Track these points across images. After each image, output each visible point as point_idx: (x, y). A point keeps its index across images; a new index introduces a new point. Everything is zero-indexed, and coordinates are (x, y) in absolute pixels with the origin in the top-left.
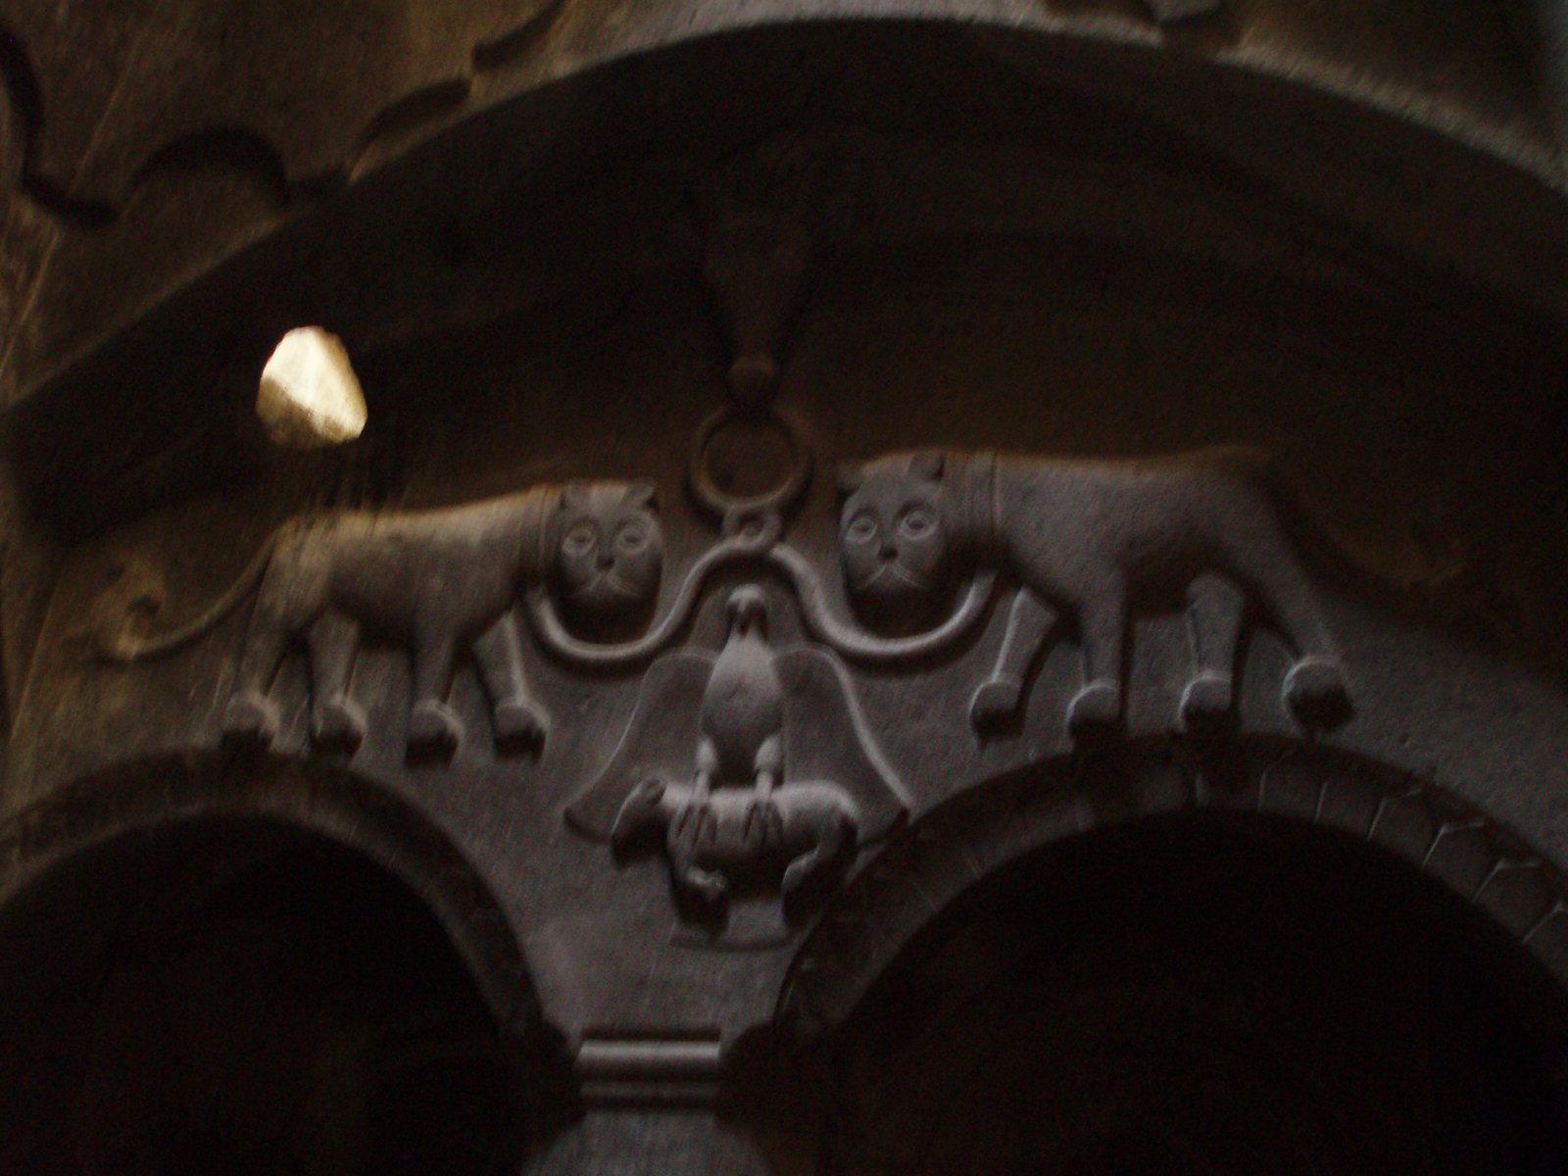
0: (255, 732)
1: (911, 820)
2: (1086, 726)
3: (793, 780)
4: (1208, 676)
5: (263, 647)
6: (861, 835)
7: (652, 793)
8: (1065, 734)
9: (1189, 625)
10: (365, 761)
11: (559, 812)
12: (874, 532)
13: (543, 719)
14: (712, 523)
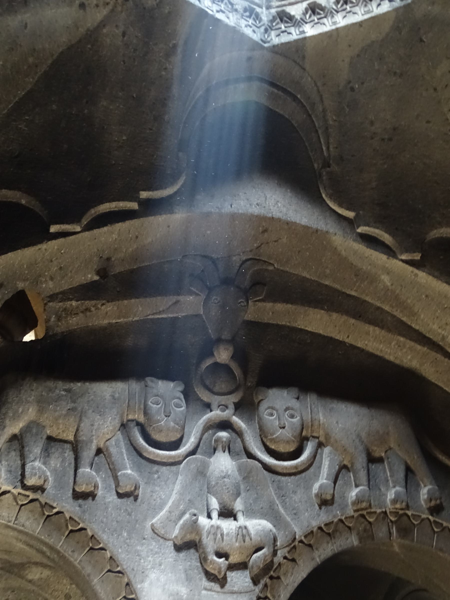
11: (148, 525)
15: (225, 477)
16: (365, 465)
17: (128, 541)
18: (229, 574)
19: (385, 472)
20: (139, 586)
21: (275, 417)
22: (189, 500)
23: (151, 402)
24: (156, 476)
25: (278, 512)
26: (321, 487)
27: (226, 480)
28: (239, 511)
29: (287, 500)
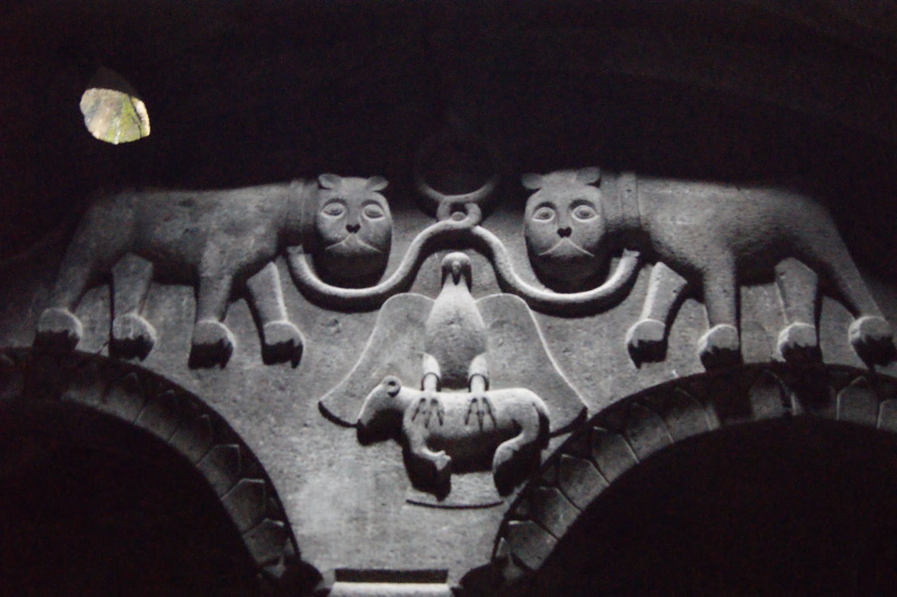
1: (589, 416)
3: (497, 387)
4: (798, 324)
5: (77, 275)
6: (552, 428)
7: (392, 389)
8: (699, 362)
9: (778, 291)
11: (313, 404)
12: (552, 219)
13: (303, 338)
14: (430, 211)
15: (452, 323)
16: (730, 288)
17: (276, 429)
18: (455, 479)
19: (774, 302)
20: (290, 497)
21: (552, 219)
22: (389, 364)
23: (326, 212)
24: (333, 329)
25: (554, 375)
26: (638, 330)
27: (453, 326)
28: (476, 375)
29: (574, 356)
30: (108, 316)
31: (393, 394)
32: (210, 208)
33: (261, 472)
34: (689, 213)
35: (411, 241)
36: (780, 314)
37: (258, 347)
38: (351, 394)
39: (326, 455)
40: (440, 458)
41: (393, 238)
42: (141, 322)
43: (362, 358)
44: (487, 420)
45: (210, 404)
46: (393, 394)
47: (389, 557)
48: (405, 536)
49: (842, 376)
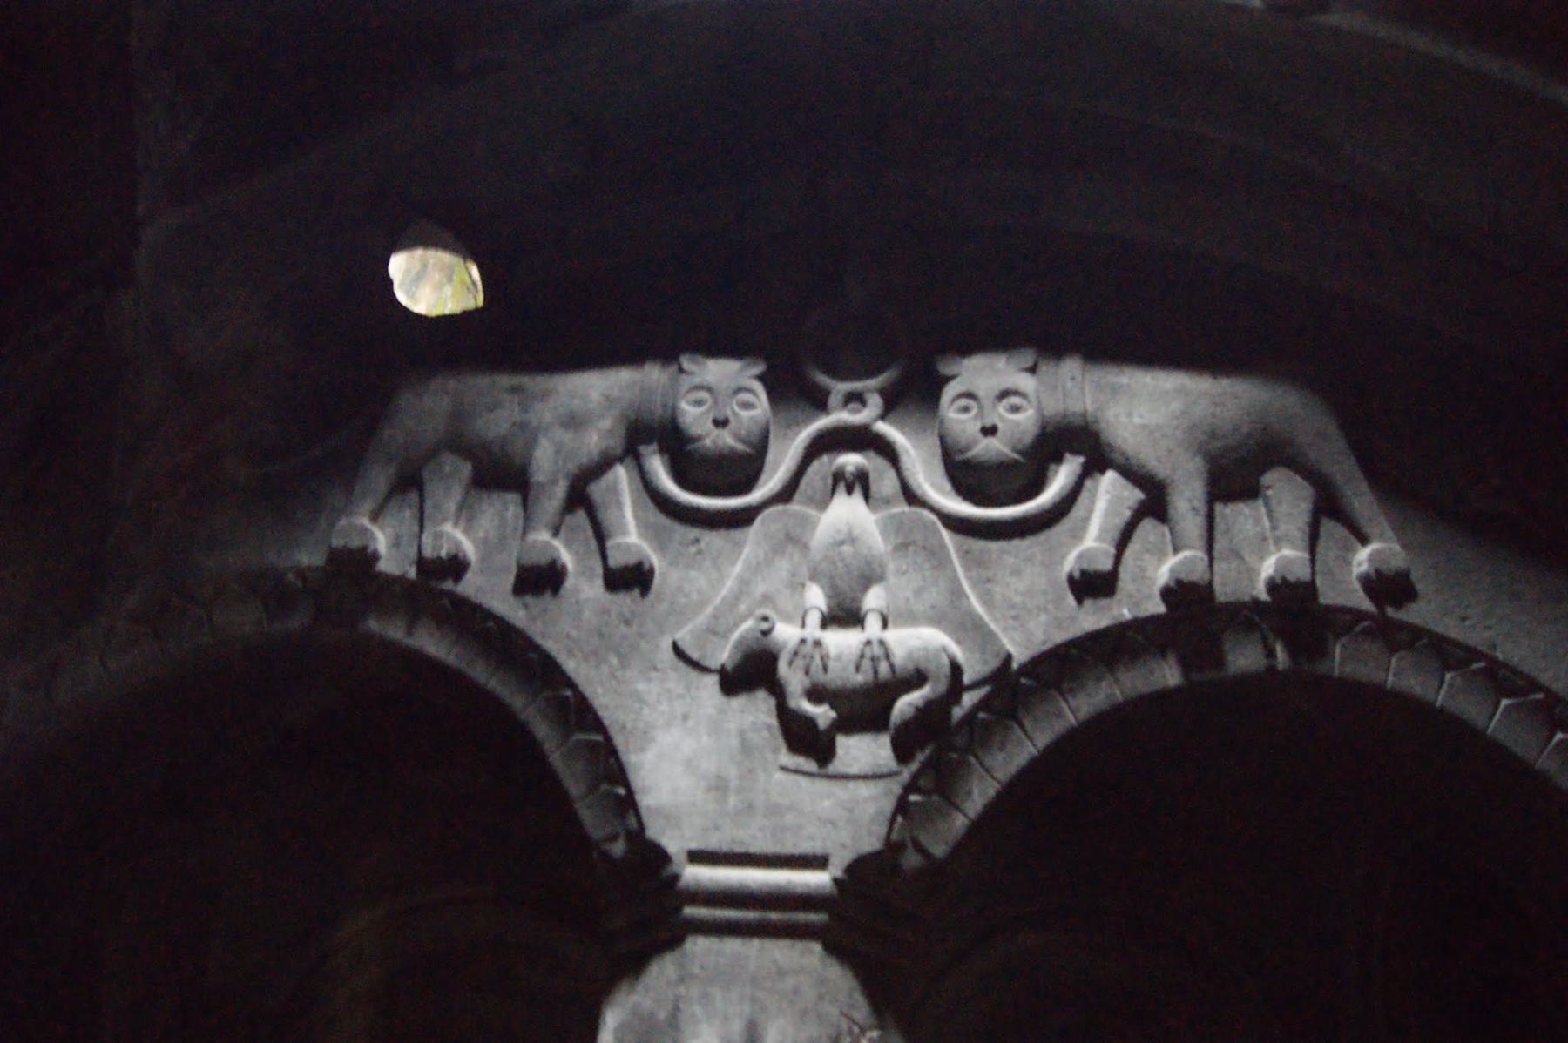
0: (365, 548)
1: (1015, 666)
2: (1177, 593)
3: (896, 625)
4: (1287, 552)
6: (967, 679)
7: (765, 626)
9: (1263, 510)
10: (470, 586)
11: (666, 644)
13: (655, 560)
14: (820, 403)
15: (842, 543)
16: (1201, 505)
19: (1257, 521)
23: (688, 403)
24: (693, 549)
25: (971, 614)
26: (1081, 557)
28: (872, 610)
29: (998, 589)
30: (416, 529)
31: (766, 633)
32: (545, 395)
33: (598, 725)
34: (1150, 408)
35: (793, 440)
36: (1265, 539)
37: (599, 570)
38: (714, 631)
39: (680, 707)
40: (823, 714)
41: (772, 436)
42: (455, 536)
43: (729, 585)
44: (884, 668)
45: (539, 640)
46: (766, 633)
47: (754, 837)
48: (774, 810)
49: (1343, 620)
